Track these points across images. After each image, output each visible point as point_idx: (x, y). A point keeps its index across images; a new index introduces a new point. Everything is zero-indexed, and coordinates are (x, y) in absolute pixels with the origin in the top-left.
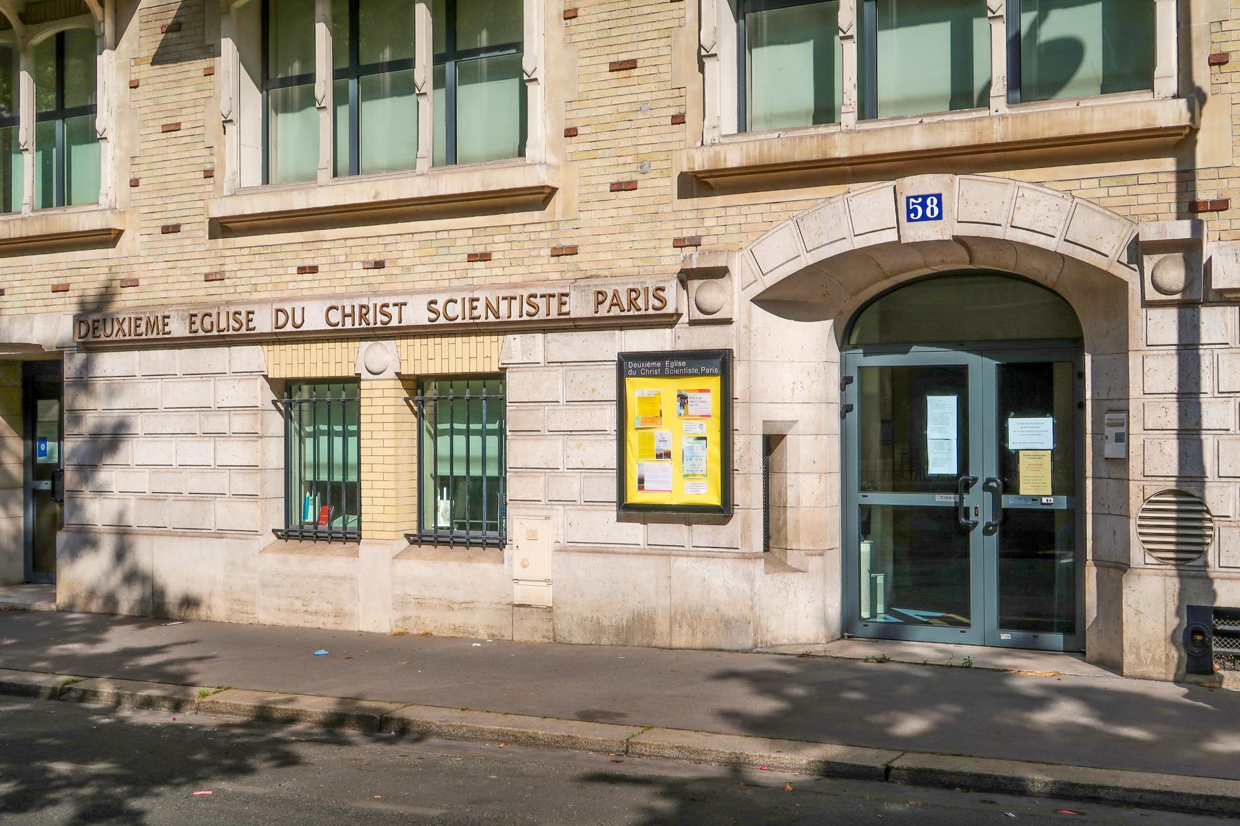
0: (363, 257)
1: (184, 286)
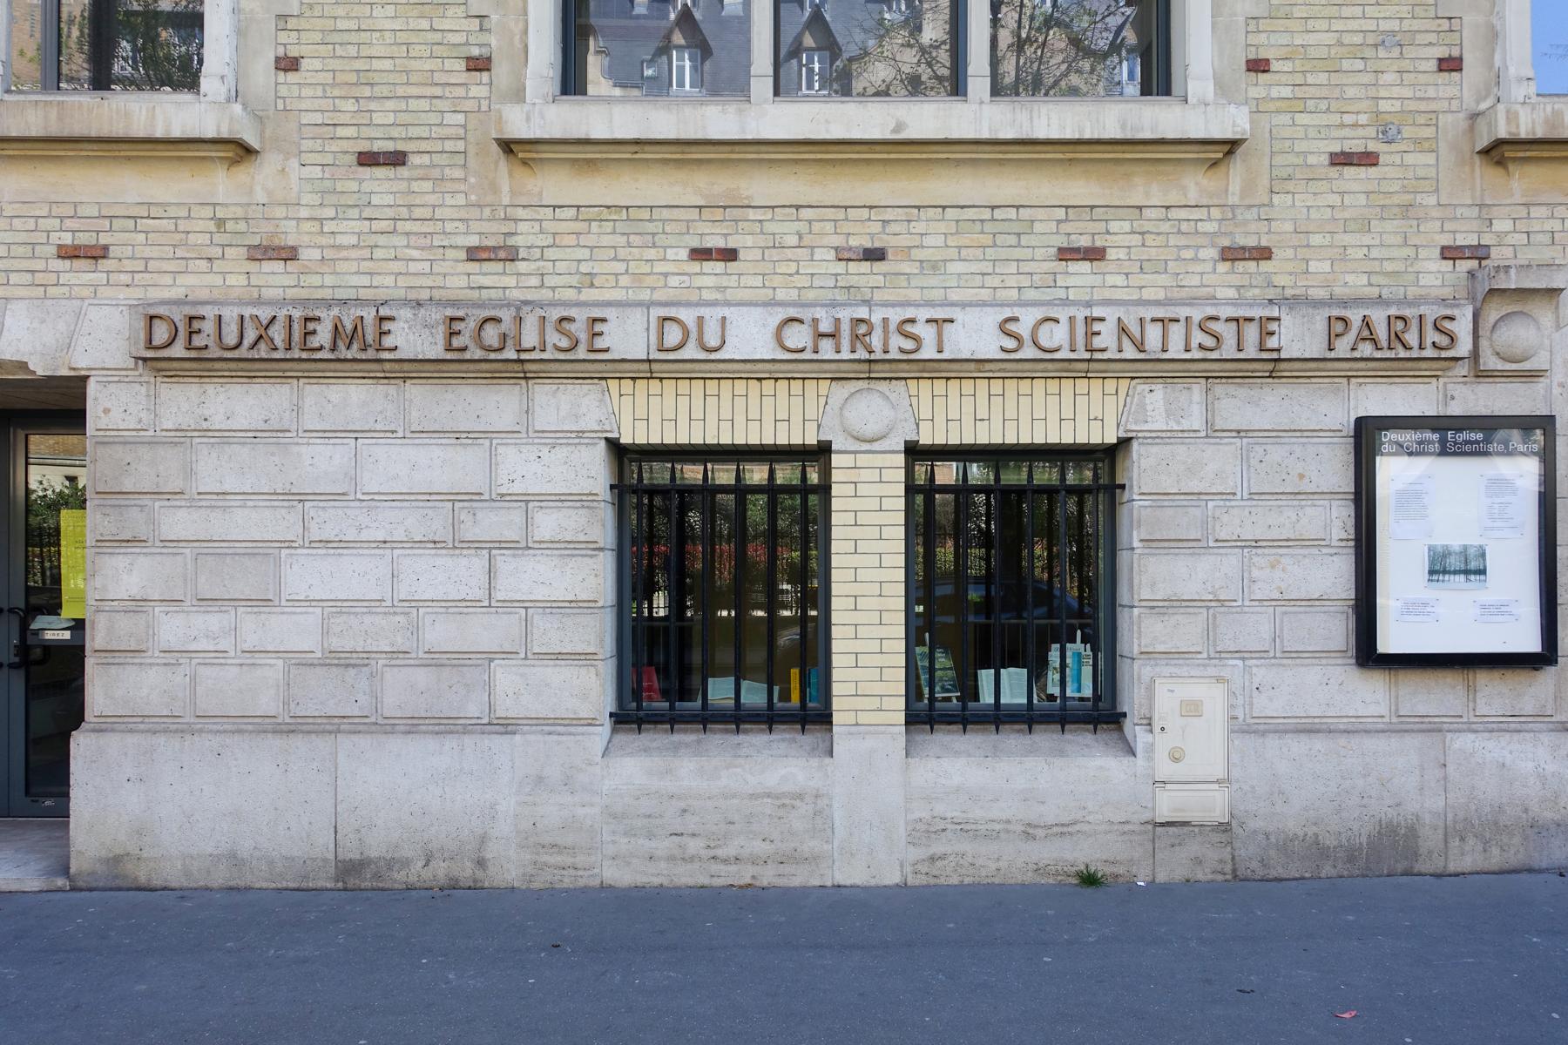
0: (838, 241)
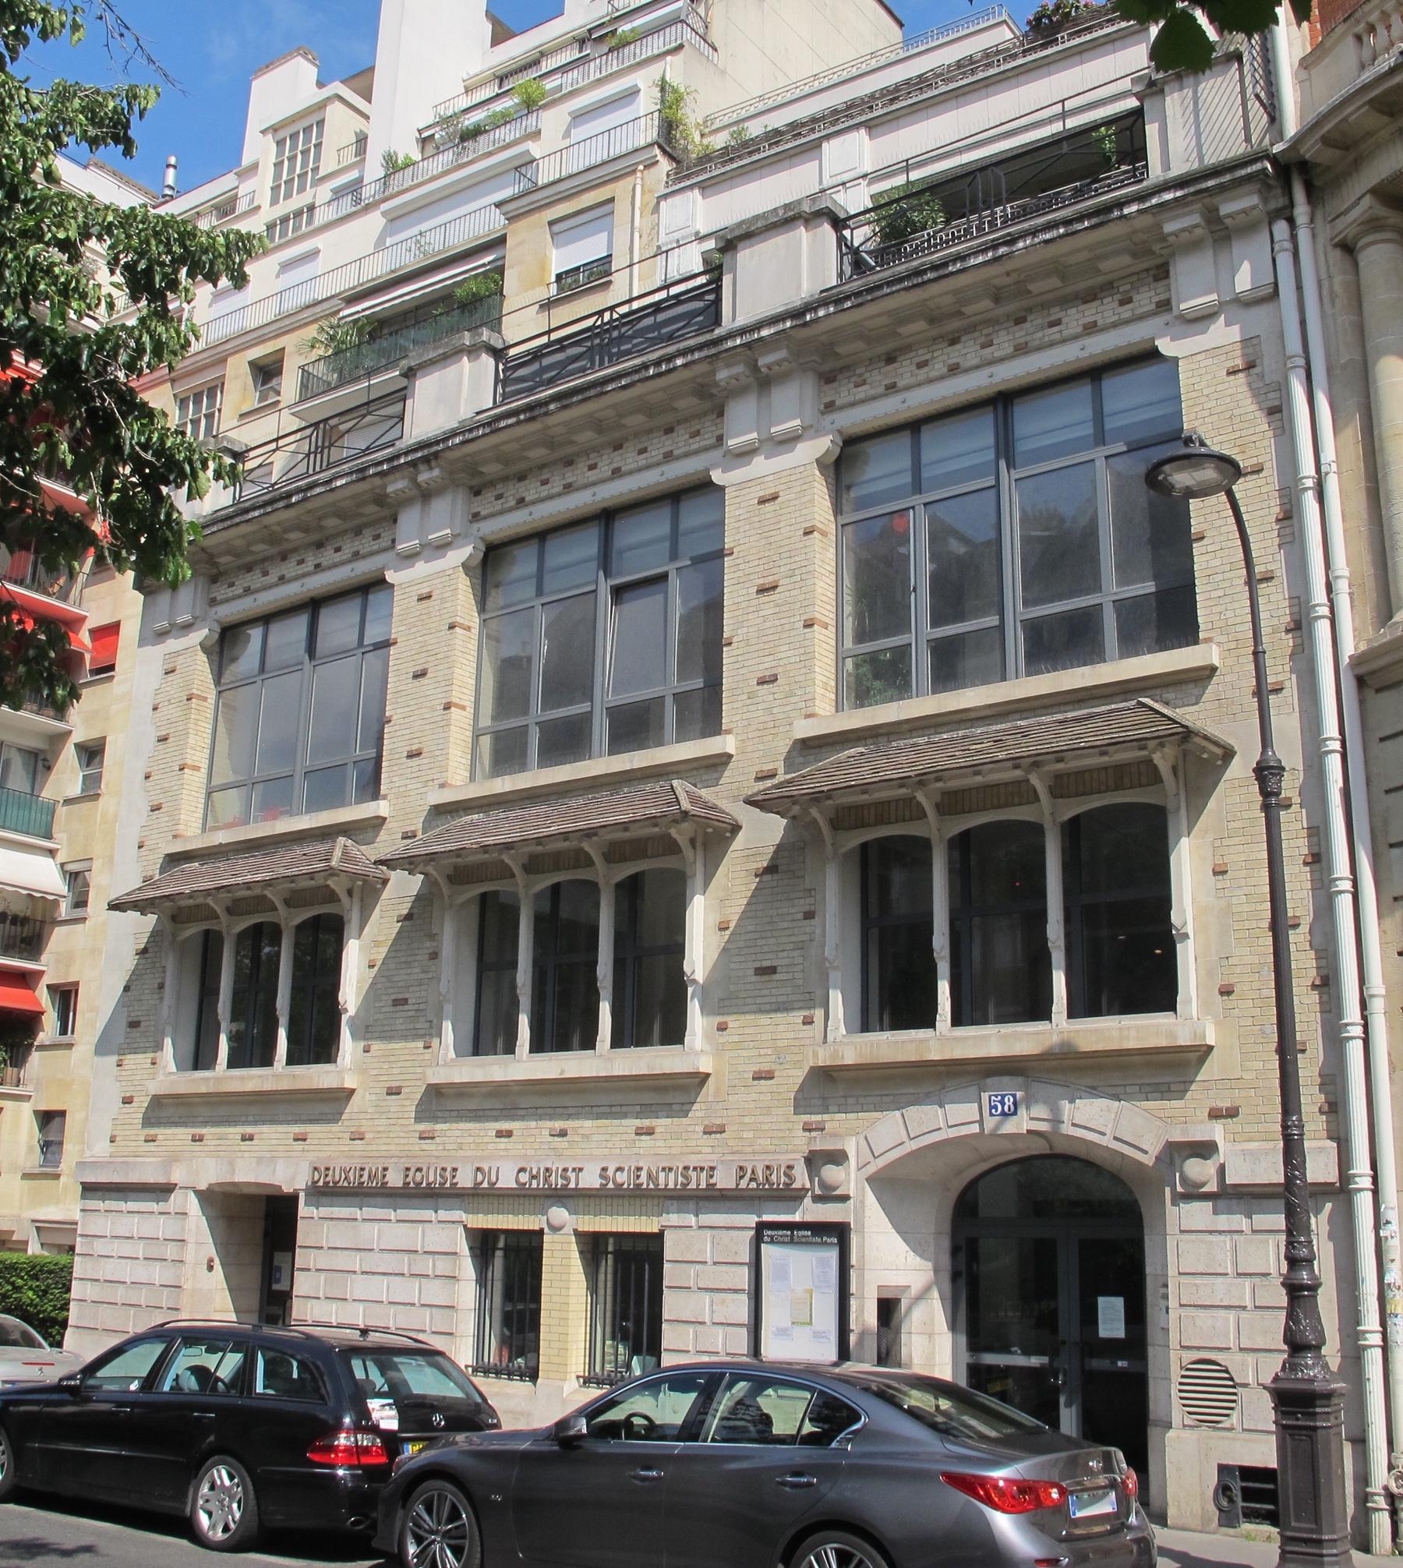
1: (403, 1141)
